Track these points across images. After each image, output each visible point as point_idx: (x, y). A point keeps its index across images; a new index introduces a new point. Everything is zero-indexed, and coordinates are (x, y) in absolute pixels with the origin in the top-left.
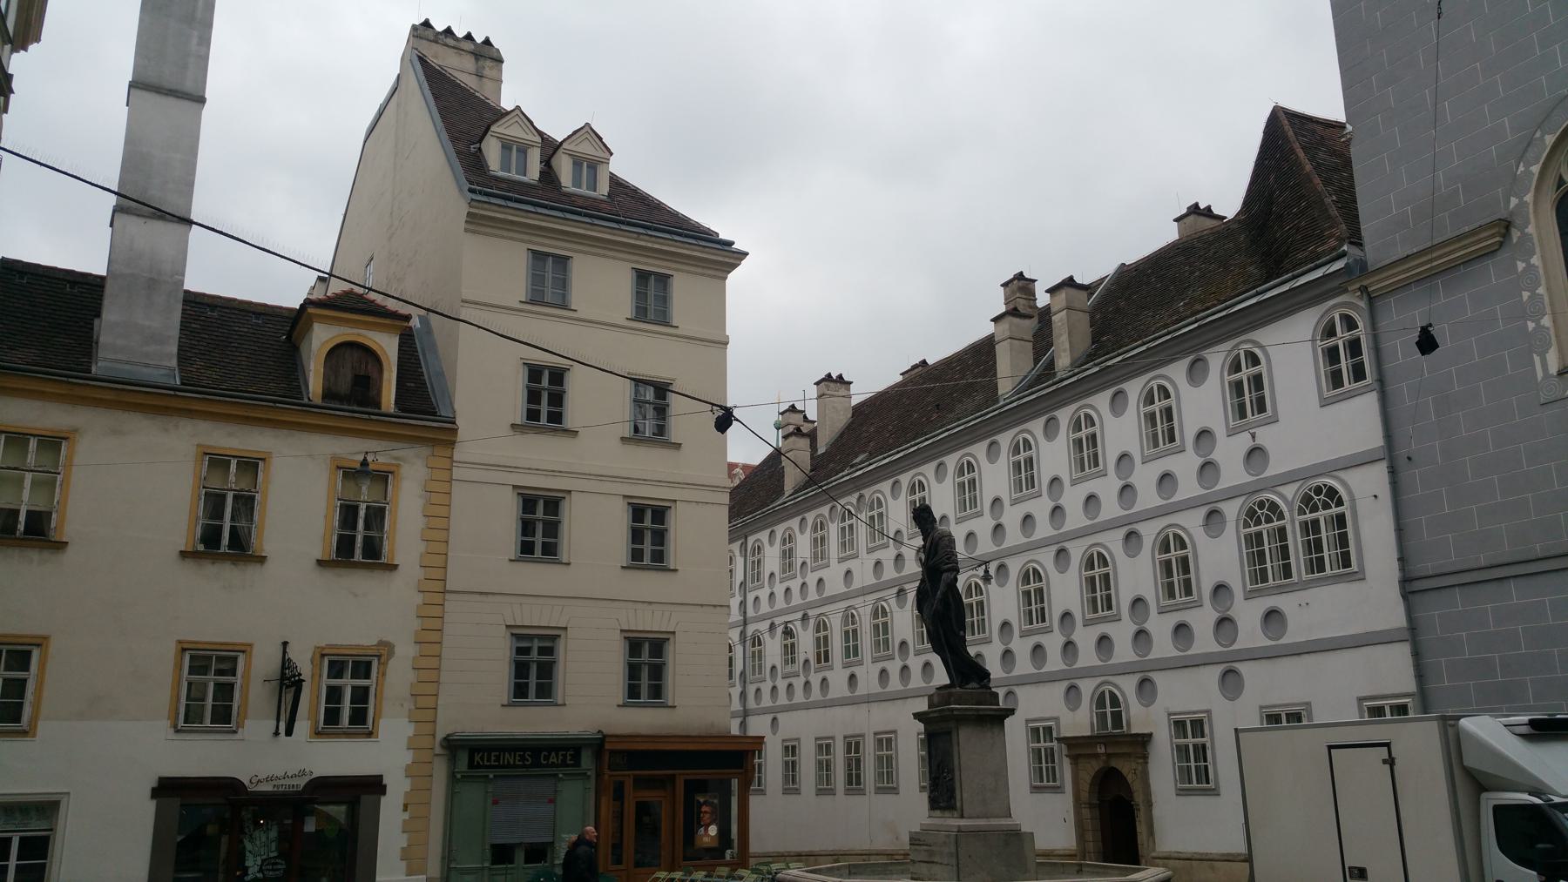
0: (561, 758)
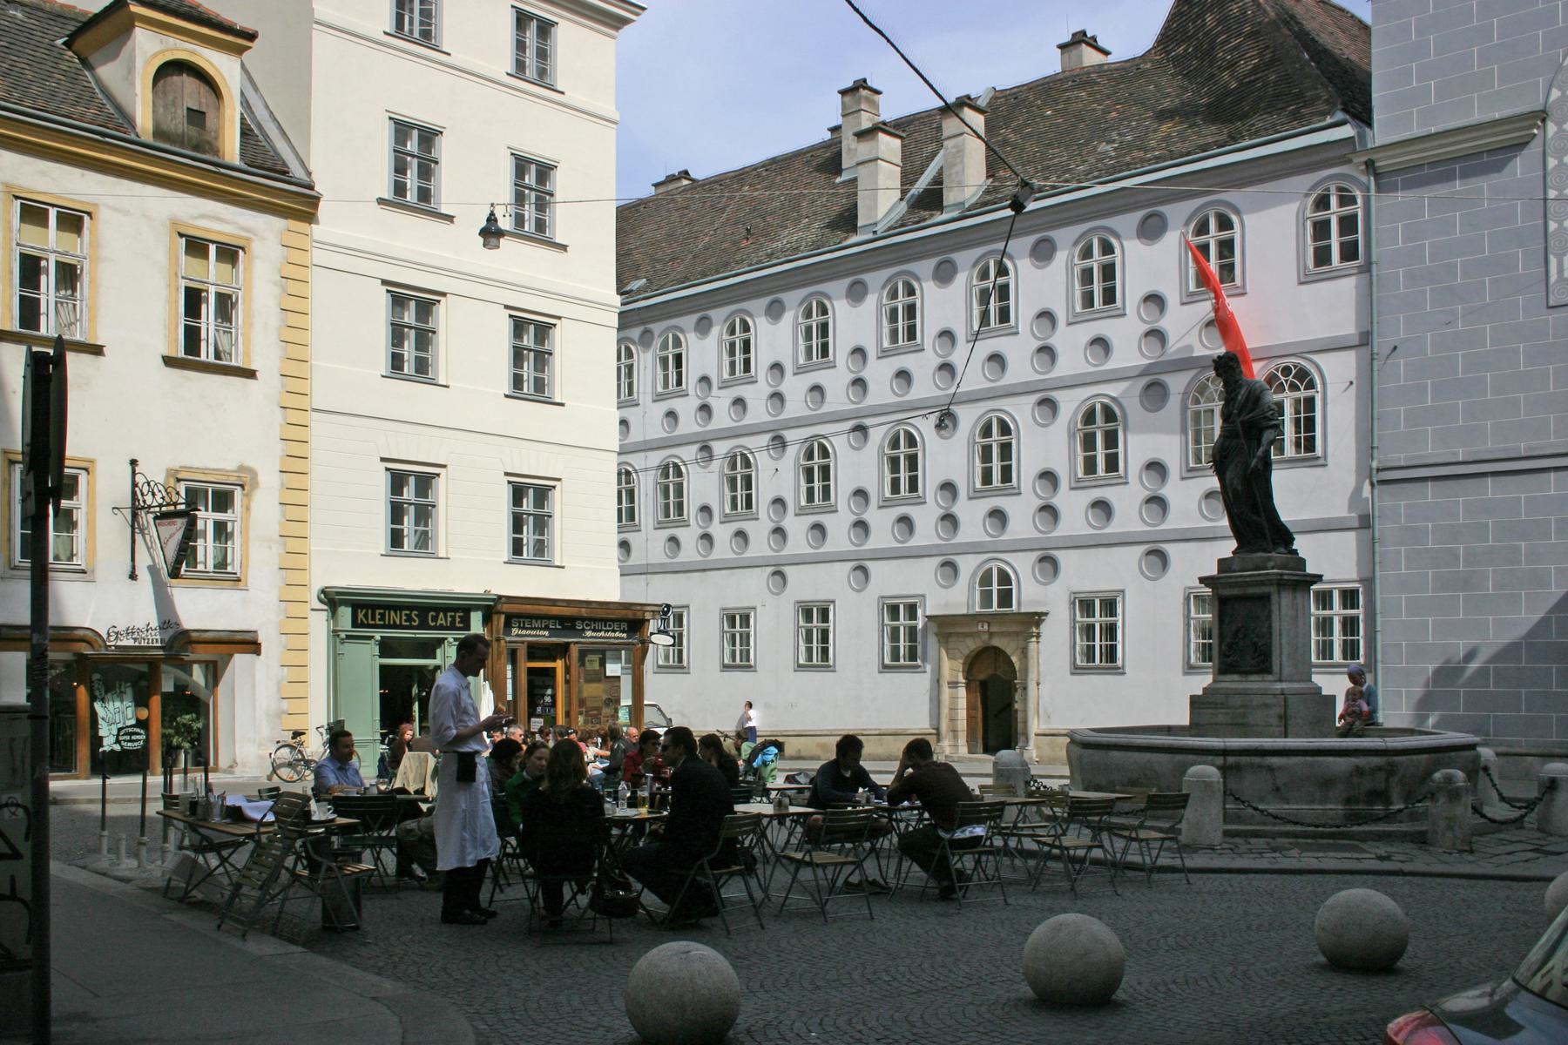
0: (449, 619)
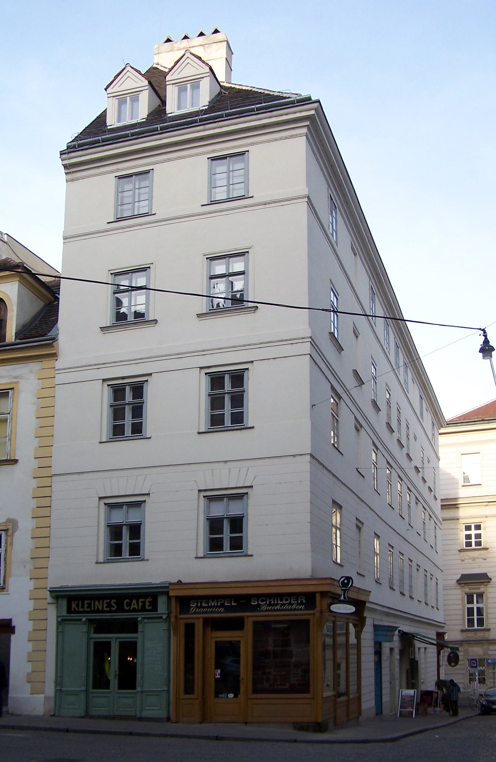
0: (140, 604)
